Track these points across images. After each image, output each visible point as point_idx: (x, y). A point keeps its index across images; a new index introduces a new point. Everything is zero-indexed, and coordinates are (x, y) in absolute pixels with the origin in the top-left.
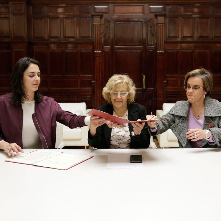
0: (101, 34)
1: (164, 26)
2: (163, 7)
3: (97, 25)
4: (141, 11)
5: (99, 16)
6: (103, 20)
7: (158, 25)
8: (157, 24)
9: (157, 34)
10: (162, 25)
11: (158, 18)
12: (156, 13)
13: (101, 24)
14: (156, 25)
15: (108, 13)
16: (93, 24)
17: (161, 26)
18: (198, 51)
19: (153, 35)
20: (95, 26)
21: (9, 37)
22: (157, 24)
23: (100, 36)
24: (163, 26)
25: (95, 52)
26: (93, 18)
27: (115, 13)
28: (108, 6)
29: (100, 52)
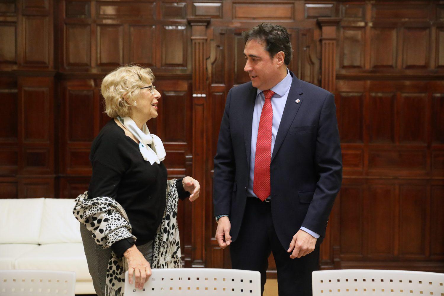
2: (332, 7)
3: (197, 41)
4: (289, 15)
7: (324, 42)
8: (321, 41)
10: (331, 42)
12: (319, 18)
13: (206, 40)
14: (318, 43)
15: (222, 18)
16: (192, 40)
17: (329, 44)
18: (404, 95)
19: (313, 63)
20: (195, 43)
21: (15, 63)
22: (321, 41)
24: (333, 44)
25: (194, 95)
26: (191, 26)
28: (222, 3)
29: (204, 95)
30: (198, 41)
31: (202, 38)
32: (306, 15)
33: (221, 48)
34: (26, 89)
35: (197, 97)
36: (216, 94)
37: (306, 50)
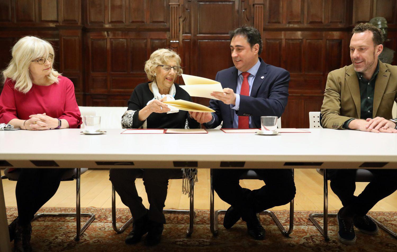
0: (179, 18)
1: (263, 7)
7: (255, 6)
8: (254, 5)
9: (254, 18)
10: (260, 6)
13: (179, 5)
14: (252, 6)
16: (169, 5)
17: (259, 7)
22: (254, 5)
25: (171, 41)
29: (177, 41)
30: (174, 6)
31: (176, 4)
33: (189, 11)
34: (64, 37)
35: (173, 42)
37: (244, 11)
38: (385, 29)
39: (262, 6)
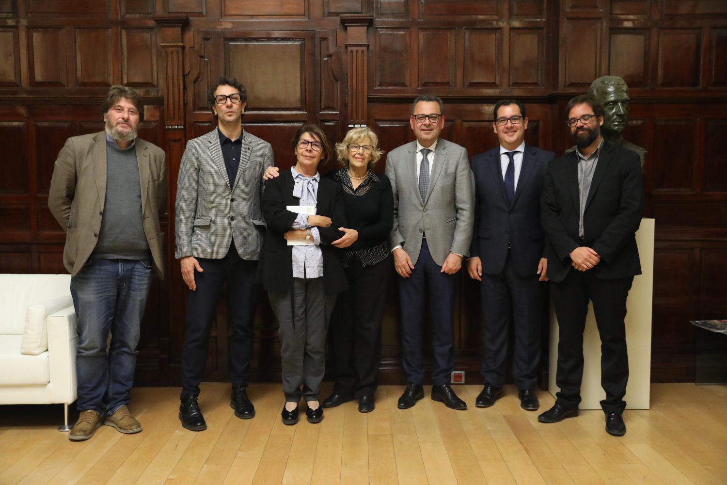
0: (184, 76)
1: (365, 52)
5: (180, 25)
6: (189, 35)
7: (349, 49)
10: (360, 49)
11: (348, 28)
14: (343, 49)
15: (206, 16)
17: (357, 51)
20: (166, 52)
23: (181, 78)
24: (363, 51)
27: (226, 15)
32: (326, 13)
36: (201, 124)
38: (623, 102)
39: (365, 48)
